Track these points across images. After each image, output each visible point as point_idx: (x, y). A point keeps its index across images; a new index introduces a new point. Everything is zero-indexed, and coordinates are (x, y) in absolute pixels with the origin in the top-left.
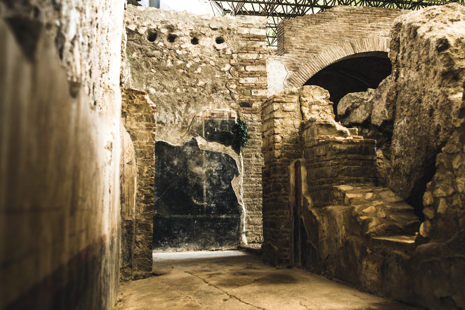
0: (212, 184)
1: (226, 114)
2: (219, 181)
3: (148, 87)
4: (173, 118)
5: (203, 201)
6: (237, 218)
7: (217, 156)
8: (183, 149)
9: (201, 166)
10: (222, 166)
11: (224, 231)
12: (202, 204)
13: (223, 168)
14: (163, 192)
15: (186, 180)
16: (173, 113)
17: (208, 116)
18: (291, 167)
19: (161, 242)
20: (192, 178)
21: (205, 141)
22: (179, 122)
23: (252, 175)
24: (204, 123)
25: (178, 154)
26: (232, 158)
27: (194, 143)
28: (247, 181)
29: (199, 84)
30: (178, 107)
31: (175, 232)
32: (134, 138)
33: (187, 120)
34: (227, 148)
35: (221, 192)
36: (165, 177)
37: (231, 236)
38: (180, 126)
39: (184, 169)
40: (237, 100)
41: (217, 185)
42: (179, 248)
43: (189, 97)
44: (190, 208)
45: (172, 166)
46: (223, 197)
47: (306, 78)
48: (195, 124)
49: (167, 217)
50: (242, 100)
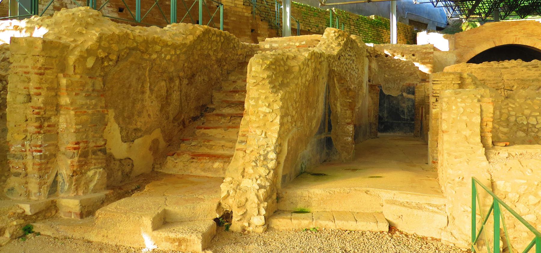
15: (398, 109)
18: (421, 109)
27: (402, 95)
32: (372, 99)
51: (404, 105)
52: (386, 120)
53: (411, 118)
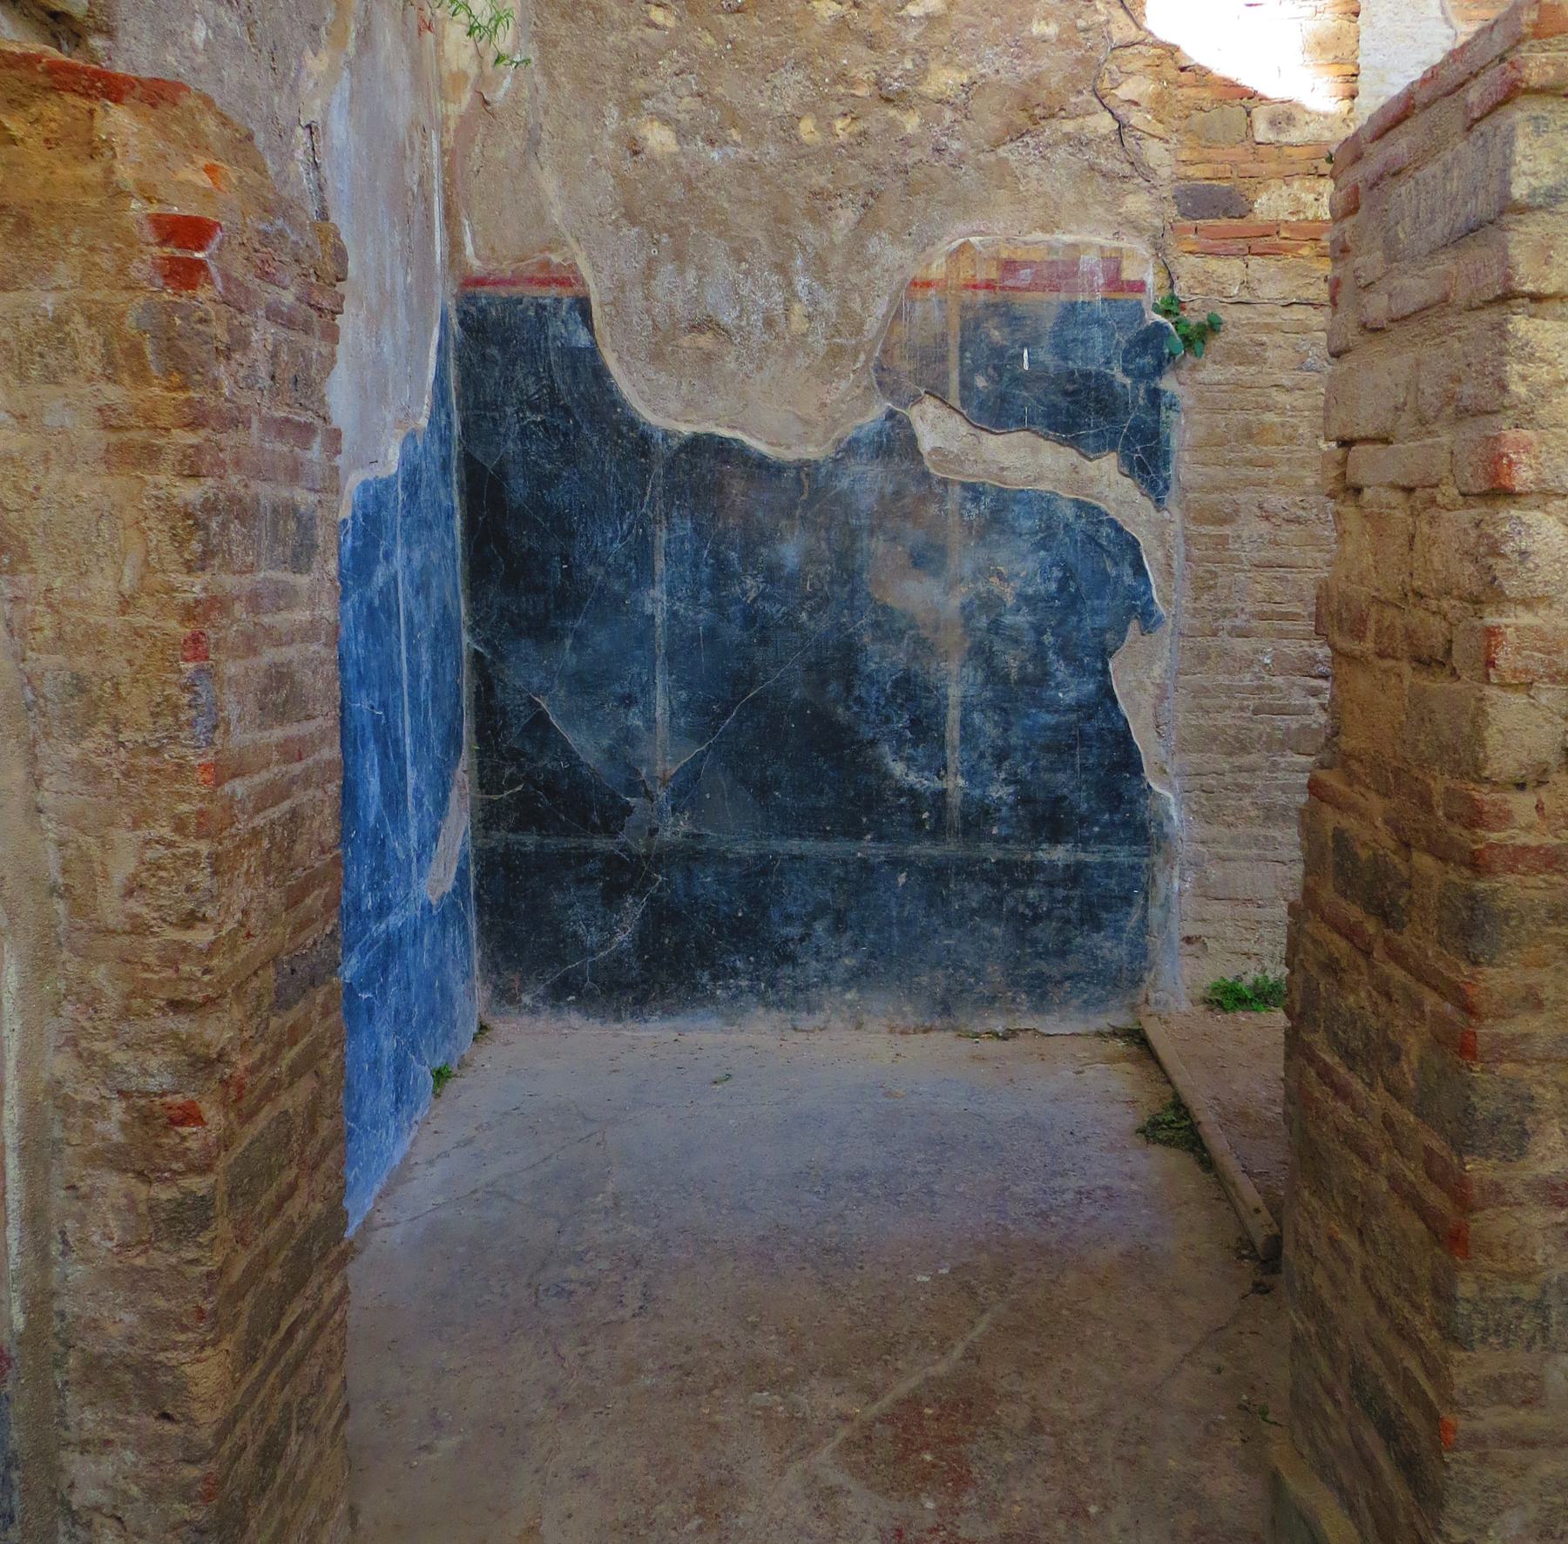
0: (994, 675)
1: (1089, 260)
2: (1039, 656)
3: (632, 121)
4: (778, 297)
5: (941, 769)
6: (1132, 868)
7: (1030, 515)
8: (831, 475)
9: (936, 574)
10: (1057, 573)
11: (1060, 931)
12: (938, 785)
13: (1062, 588)
14: (726, 713)
15: (849, 651)
16: (782, 269)
17: (981, 276)
19: (714, 978)
20: (884, 638)
21: (964, 429)
22: (810, 317)
23: (1238, 622)
24: (956, 322)
25: (809, 504)
26: (1119, 530)
27: (896, 443)
28: (1203, 657)
29: (930, 88)
30: (809, 233)
31: (794, 931)
33: (856, 305)
34: (1091, 468)
35: (1048, 719)
36: (733, 632)
37: (1095, 959)
38: (820, 344)
39: (843, 593)
40: (1164, 172)
41: (1023, 680)
42: (810, 1011)
43: (875, 168)
44: (863, 803)
45: (772, 573)
46: (1062, 746)
48: (901, 330)
49: (747, 849)
50: (1191, 171)
51: (932, 601)
52: (675, 829)
53: (1025, 800)
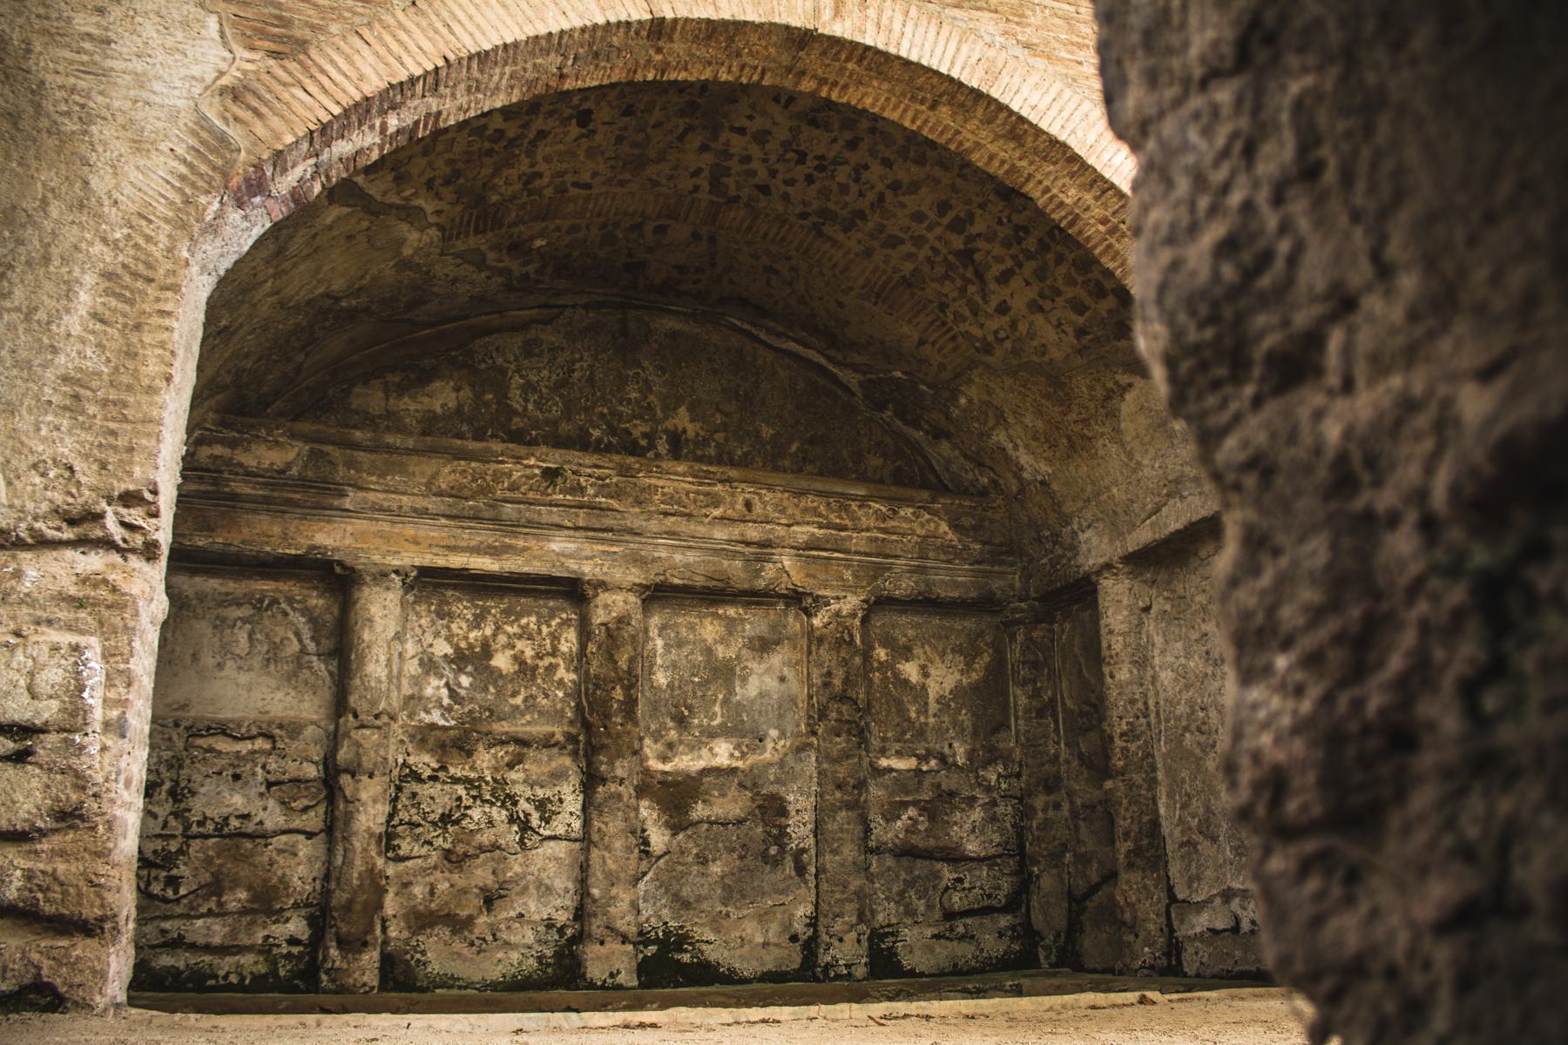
47: (340, 96)
